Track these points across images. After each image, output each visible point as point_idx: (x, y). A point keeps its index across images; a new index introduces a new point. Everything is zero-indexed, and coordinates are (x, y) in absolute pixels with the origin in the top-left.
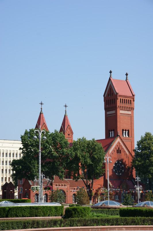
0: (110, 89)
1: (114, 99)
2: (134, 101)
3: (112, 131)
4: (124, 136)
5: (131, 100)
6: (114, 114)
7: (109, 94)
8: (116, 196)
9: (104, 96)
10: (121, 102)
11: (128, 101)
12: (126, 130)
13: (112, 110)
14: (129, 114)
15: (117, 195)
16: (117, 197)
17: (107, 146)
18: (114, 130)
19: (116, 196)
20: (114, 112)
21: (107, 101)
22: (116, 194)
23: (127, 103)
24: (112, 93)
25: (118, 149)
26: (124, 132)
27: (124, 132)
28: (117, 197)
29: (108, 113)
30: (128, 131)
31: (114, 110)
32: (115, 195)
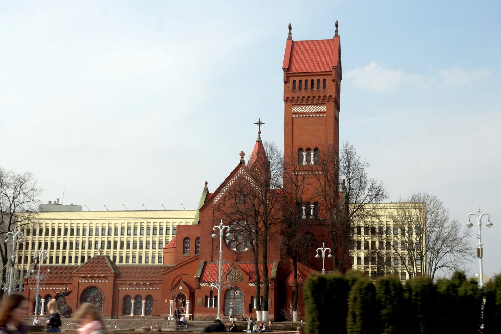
4: (304, 163)
5: (324, 80)
8: (209, 299)
10: (294, 88)
11: (315, 82)
12: (308, 150)
14: (320, 113)
15: (211, 297)
16: (211, 300)
17: (348, 192)
19: (209, 299)
22: (208, 295)
23: (312, 88)
26: (304, 154)
27: (304, 154)
28: (211, 300)
30: (316, 150)
32: (206, 297)
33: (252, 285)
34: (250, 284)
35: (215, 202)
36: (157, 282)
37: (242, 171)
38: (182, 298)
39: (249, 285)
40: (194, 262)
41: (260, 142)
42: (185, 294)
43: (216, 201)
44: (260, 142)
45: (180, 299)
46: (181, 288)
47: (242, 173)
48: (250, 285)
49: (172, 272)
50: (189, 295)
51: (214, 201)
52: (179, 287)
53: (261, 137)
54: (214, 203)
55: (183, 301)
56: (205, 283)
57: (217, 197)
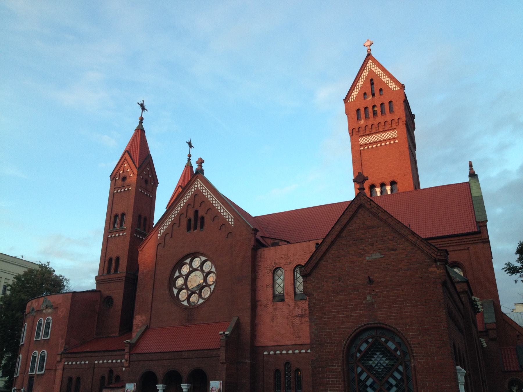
0: (372, 80)
1: (390, 102)
2: (414, 129)
3: (383, 185)
6: (394, 139)
7: (365, 94)
9: (346, 100)
13: (385, 131)
18: (393, 183)
20: (393, 134)
21: (358, 110)
24: (381, 90)
29: (364, 140)
31: (395, 129)
41: (140, 131)
44: (140, 131)
53: (143, 124)
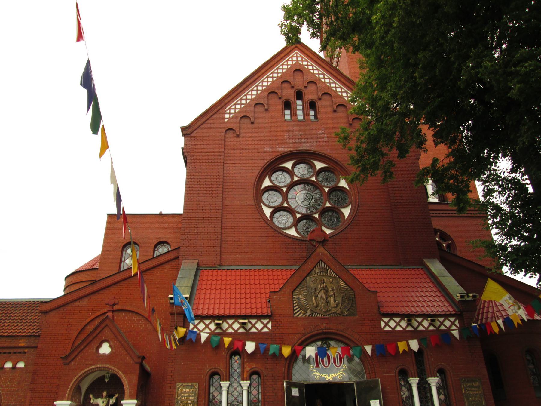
25: (290, 95)
33: (392, 324)
34: (386, 320)
35: (230, 114)
36: (22, 343)
37: (297, 57)
38: (105, 394)
39: (383, 324)
40: (156, 270)
42: (121, 374)
43: (232, 111)
45: (96, 397)
46: (105, 349)
47: (297, 61)
48: (387, 324)
49: (77, 304)
50: (135, 378)
51: (228, 112)
52: (100, 346)
54: (227, 116)
55: (108, 402)
56: (207, 322)
57: (235, 104)
